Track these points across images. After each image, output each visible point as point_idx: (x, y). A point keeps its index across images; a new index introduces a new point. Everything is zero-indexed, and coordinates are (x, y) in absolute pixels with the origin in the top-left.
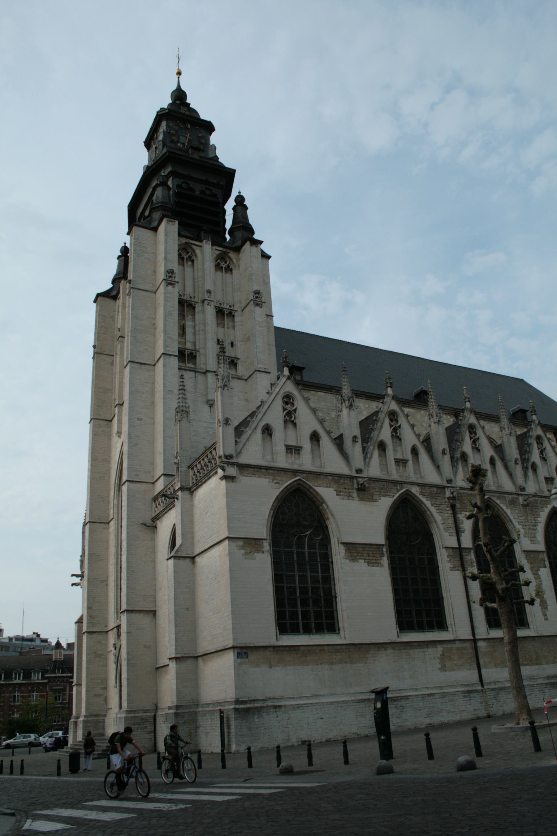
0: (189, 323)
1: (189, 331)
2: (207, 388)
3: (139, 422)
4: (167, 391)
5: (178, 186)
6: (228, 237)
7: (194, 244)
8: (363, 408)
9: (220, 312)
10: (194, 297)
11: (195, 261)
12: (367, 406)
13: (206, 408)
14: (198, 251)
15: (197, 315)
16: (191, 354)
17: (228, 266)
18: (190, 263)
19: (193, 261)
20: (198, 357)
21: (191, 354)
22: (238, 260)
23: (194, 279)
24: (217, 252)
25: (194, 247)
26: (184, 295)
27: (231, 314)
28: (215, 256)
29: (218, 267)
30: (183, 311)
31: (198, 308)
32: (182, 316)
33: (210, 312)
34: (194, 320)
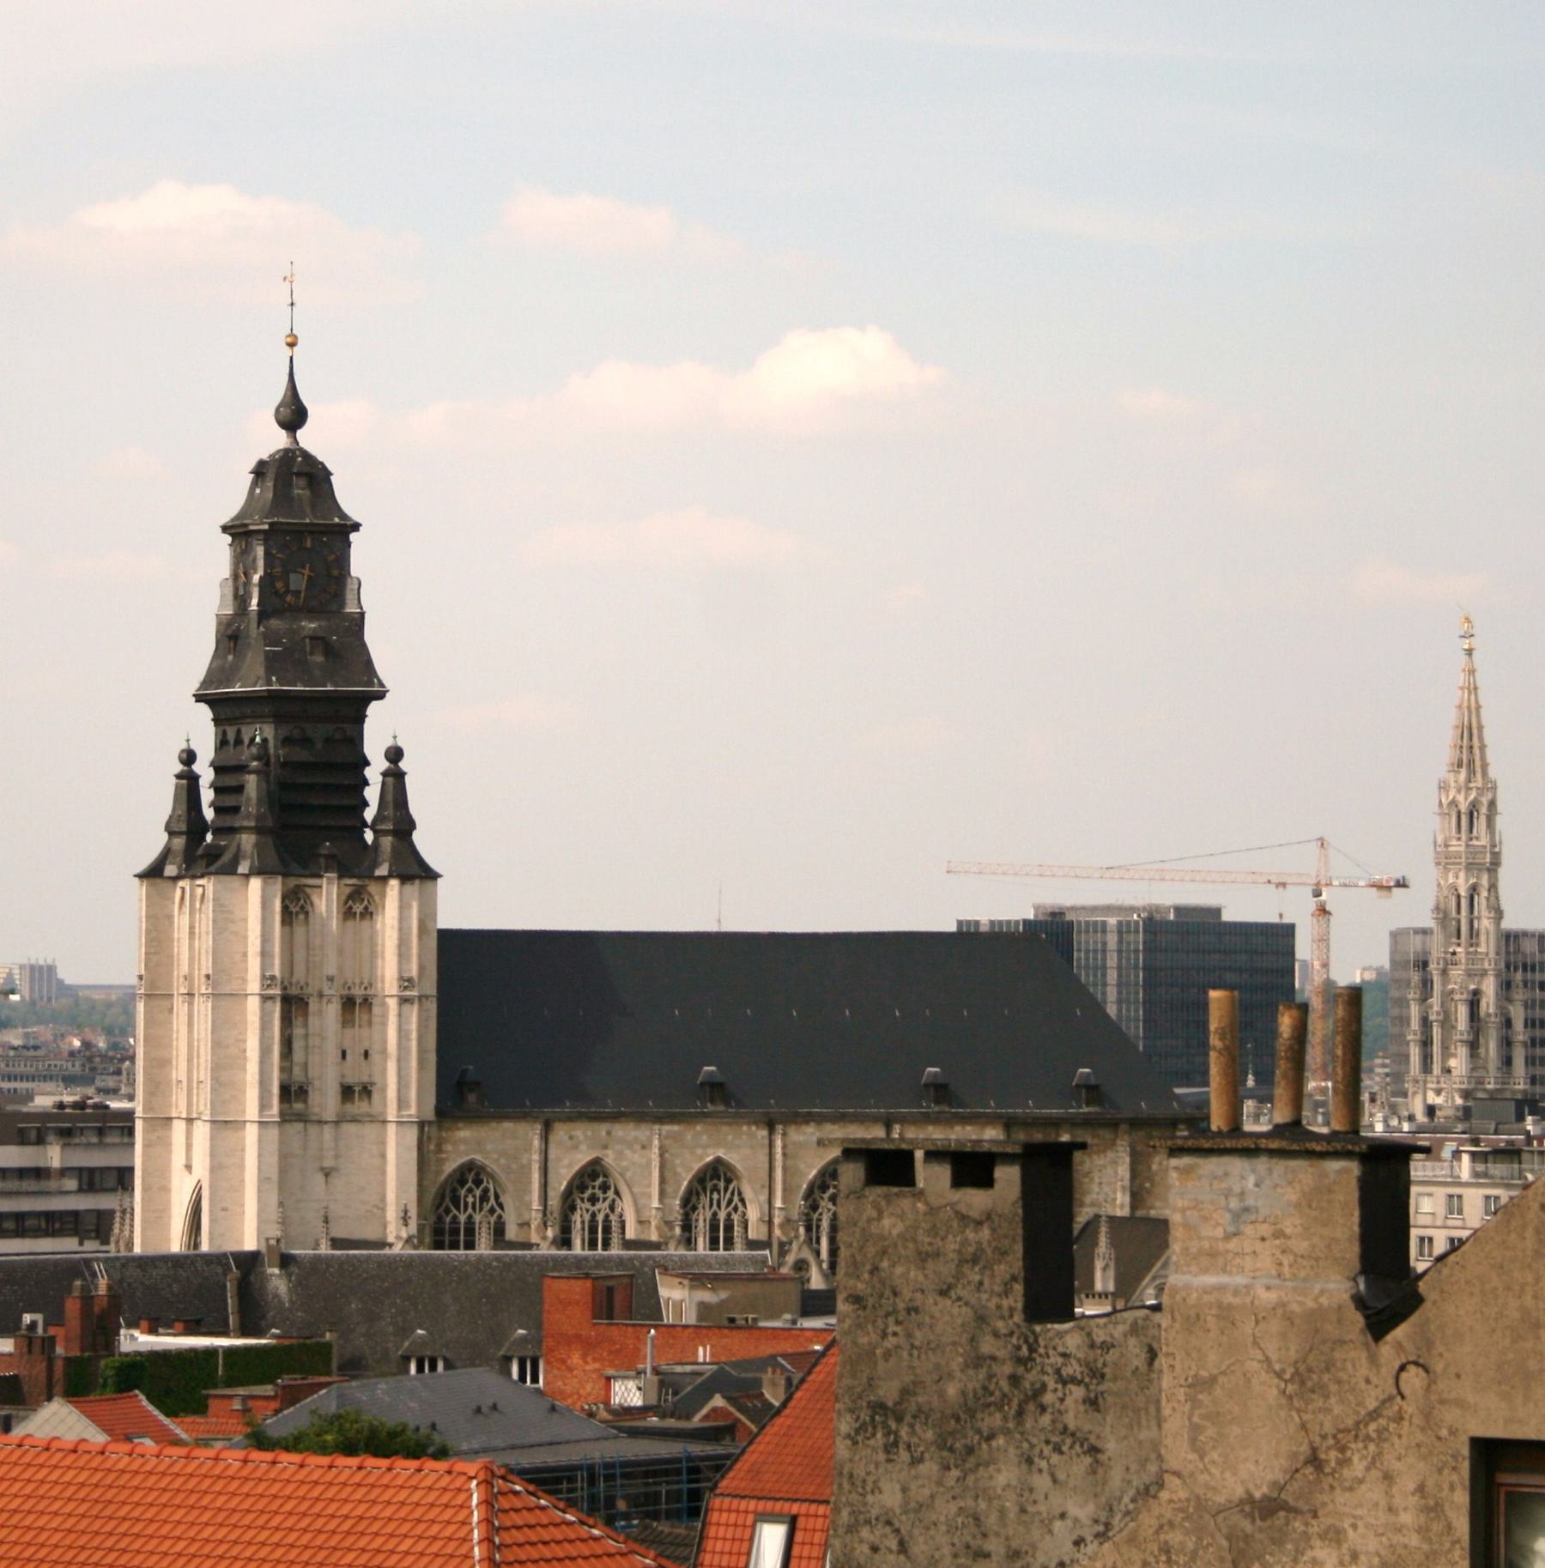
0: (298, 1031)
1: (298, 1045)
2: (321, 1149)
3: (223, 1214)
4: (263, 1180)
5: (286, 741)
6: (369, 836)
7: (309, 886)
8: (581, 1138)
9: (349, 1003)
10: (307, 984)
11: (311, 914)
12: (589, 1133)
13: (320, 1178)
14: (315, 899)
15: (311, 1019)
16: (301, 1088)
17: (366, 908)
18: (301, 917)
19: (307, 913)
20: (310, 1093)
21: (301, 1088)
22: (383, 895)
23: (308, 948)
24: (348, 890)
25: (308, 890)
26: (291, 984)
27: (367, 1002)
28: (343, 898)
29: (348, 914)
30: (290, 1011)
31: (313, 1006)
32: (286, 1021)
33: (333, 1010)
34: (306, 1025)
